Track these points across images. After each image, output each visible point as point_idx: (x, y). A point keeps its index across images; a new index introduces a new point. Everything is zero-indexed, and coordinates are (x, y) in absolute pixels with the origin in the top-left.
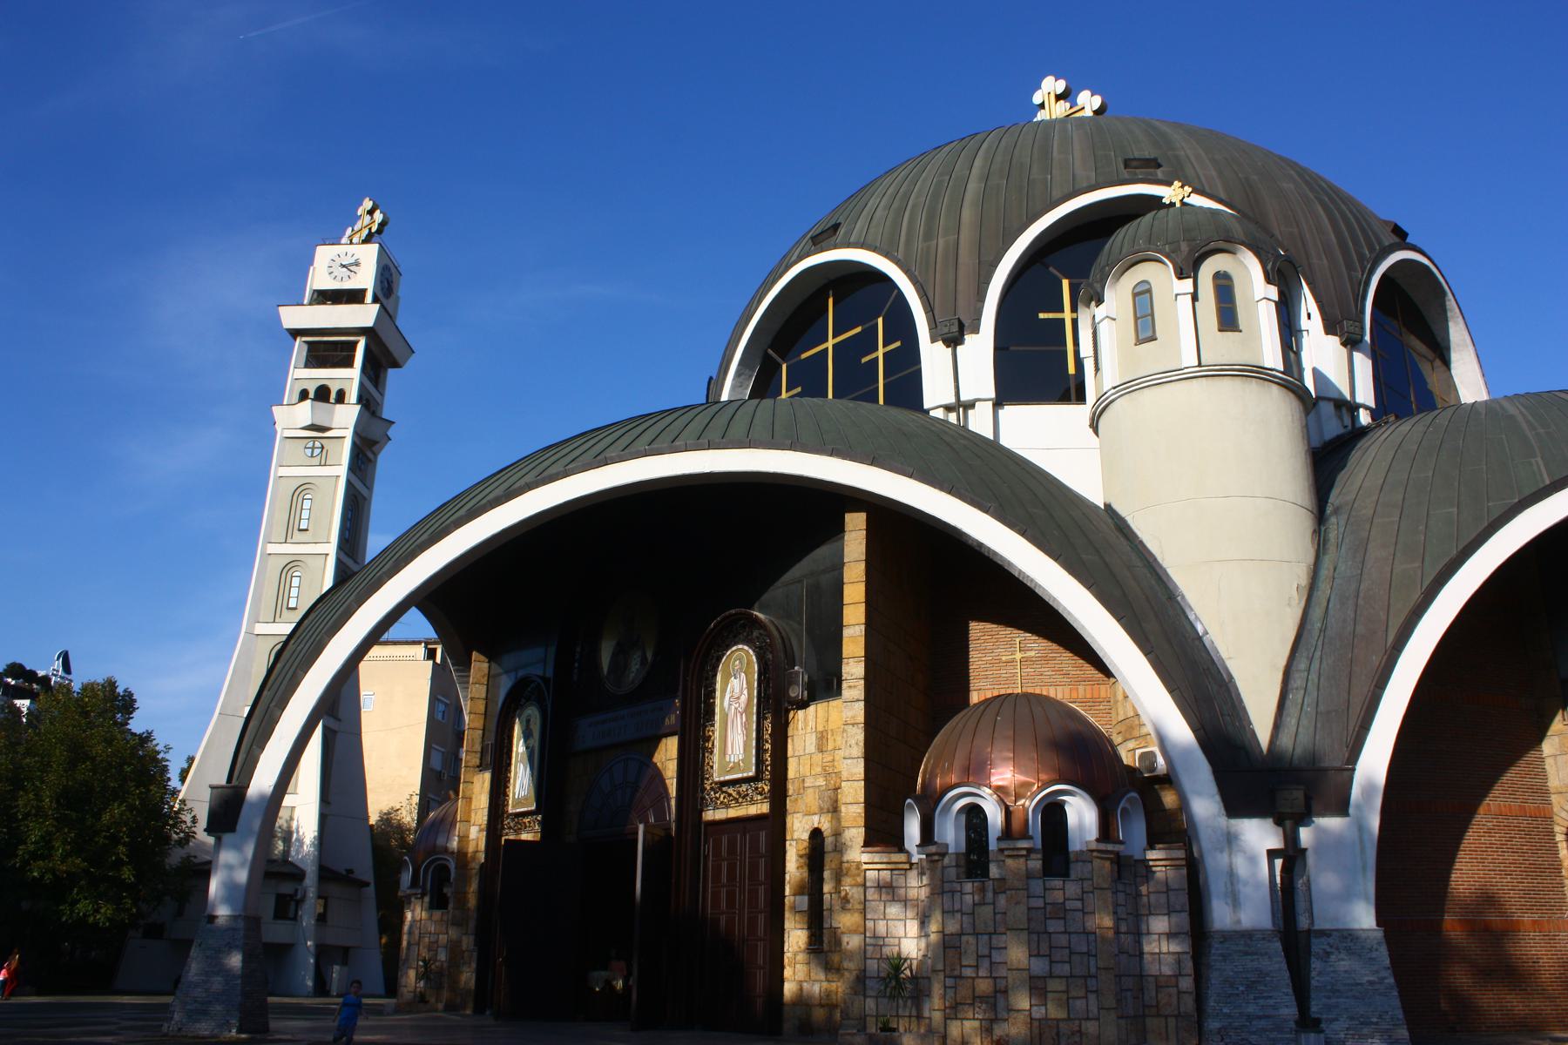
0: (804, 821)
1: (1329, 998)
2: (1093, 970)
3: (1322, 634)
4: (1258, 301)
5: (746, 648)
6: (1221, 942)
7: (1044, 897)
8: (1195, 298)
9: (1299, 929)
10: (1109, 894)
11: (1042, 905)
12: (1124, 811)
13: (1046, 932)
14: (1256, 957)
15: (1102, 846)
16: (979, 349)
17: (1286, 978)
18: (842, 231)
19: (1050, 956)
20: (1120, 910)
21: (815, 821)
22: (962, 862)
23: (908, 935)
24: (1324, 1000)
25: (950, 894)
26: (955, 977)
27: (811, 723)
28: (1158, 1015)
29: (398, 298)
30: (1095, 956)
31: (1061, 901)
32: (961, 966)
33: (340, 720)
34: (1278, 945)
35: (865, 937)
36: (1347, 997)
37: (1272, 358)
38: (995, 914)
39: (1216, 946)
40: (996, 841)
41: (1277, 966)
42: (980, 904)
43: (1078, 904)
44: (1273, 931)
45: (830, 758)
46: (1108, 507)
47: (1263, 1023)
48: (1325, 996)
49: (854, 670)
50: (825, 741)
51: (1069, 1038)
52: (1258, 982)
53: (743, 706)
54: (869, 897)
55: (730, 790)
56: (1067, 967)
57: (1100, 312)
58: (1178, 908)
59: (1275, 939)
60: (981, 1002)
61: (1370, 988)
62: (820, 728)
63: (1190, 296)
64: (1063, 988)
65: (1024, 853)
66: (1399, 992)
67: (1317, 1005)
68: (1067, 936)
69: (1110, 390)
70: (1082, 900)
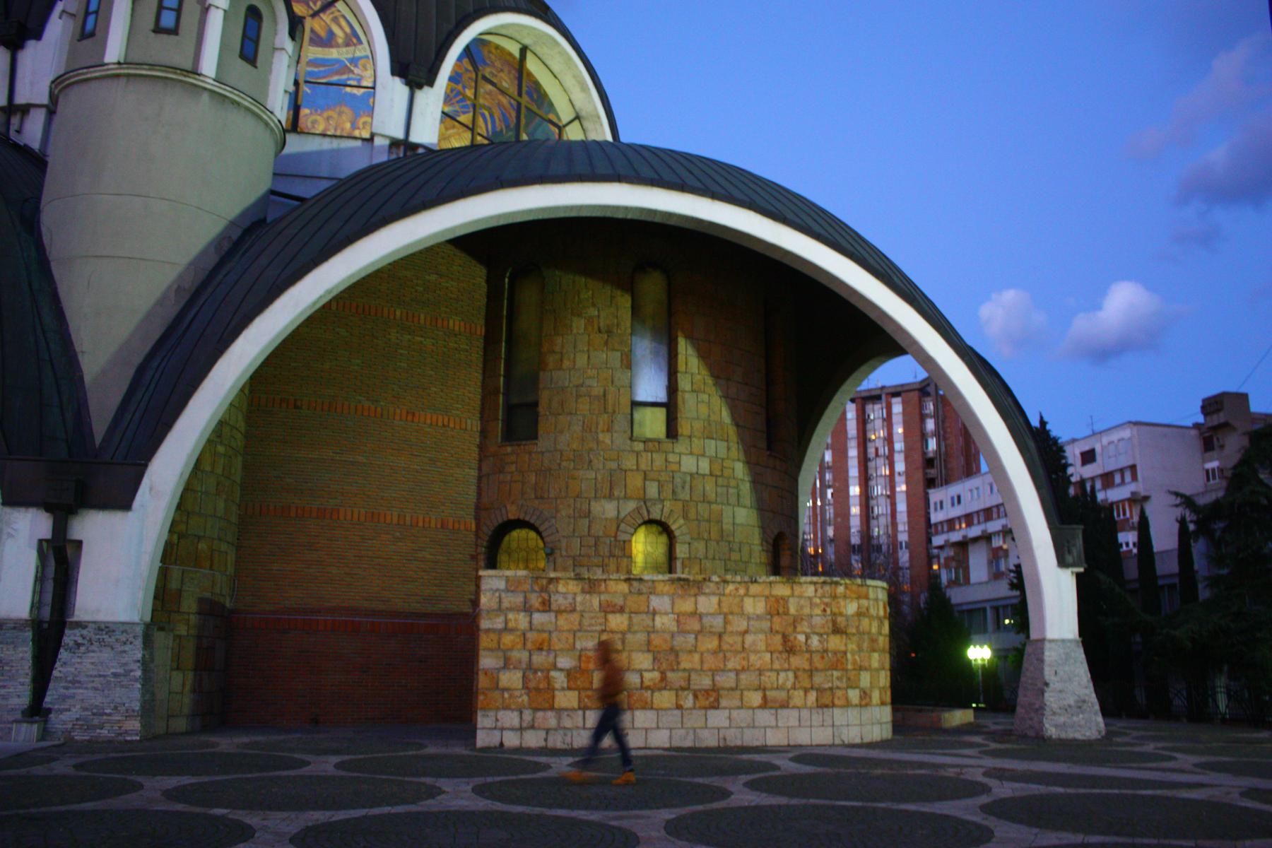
1: (67, 688)
17: (27, 667)
24: (63, 691)
34: (29, 634)
36: (86, 688)
61: (112, 680)
66: (143, 685)
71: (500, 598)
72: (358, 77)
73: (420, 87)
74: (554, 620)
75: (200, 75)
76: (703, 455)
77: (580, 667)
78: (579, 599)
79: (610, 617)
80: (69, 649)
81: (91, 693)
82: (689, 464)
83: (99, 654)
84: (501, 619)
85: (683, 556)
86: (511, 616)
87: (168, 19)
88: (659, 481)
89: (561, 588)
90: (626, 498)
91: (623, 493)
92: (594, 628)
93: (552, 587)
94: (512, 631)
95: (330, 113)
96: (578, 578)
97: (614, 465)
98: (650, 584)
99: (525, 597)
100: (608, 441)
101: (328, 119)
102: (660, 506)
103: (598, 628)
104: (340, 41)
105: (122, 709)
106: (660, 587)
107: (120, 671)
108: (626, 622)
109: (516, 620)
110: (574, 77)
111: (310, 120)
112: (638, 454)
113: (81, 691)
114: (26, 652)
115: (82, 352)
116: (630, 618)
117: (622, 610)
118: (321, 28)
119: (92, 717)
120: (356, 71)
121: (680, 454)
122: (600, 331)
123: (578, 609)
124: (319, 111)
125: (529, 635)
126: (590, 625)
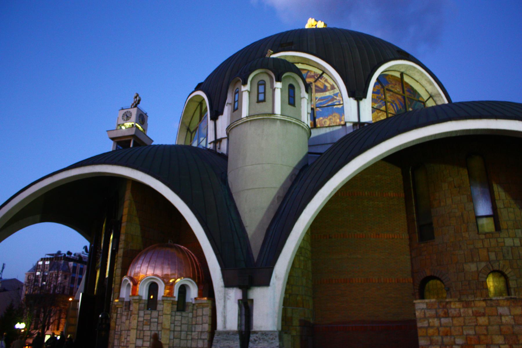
10: (169, 316)
14: (229, 341)
19: (143, 339)
29: (147, 124)
31: (149, 318)
34: (238, 337)
35: (115, 331)
41: (236, 345)
43: (156, 320)
54: (118, 317)
58: (205, 322)
59: (237, 334)
65: (137, 301)
68: (150, 332)
71: (424, 312)
72: (339, 101)
73: (361, 99)
74: (451, 321)
75: (275, 114)
76: (516, 237)
77: (467, 343)
78: (462, 310)
79: (479, 318)
80: (252, 342)
82: (509, 242)
83: (263, 344)
84: (426, 322)
85: (514, 286)
86: (430, 320)
87: (261, 97)
88: (495, 252)
89: (453, 306)
90: (480, 261)
91: (479, 259)
92: (471, 324)
93: (448, 306)
94: (433, 327)
95: (331, 117)
96: (460, 301)
97: (472, 247)
98: (496, 301)
99: (436, 312)
100: (468, 236)
101: (330, 119)
102: (498, 264)
103: (474, 324)
104: (329, 88)
106: (501, 303)
108: (487, 321)
109: (433, 322)
110: (426, 80)
111: (323, 122)
112: (482, 240)
114: (237, 343)
115: (247, 226)
116: (489, 319)
117: (484, 315)
118: (321, 85)
120: (337, 98)
121: (504, 238)
122: (455, 187)
123: (462, 315)
124: (326, 117)
125: (440, 329)
126: (469, 323)
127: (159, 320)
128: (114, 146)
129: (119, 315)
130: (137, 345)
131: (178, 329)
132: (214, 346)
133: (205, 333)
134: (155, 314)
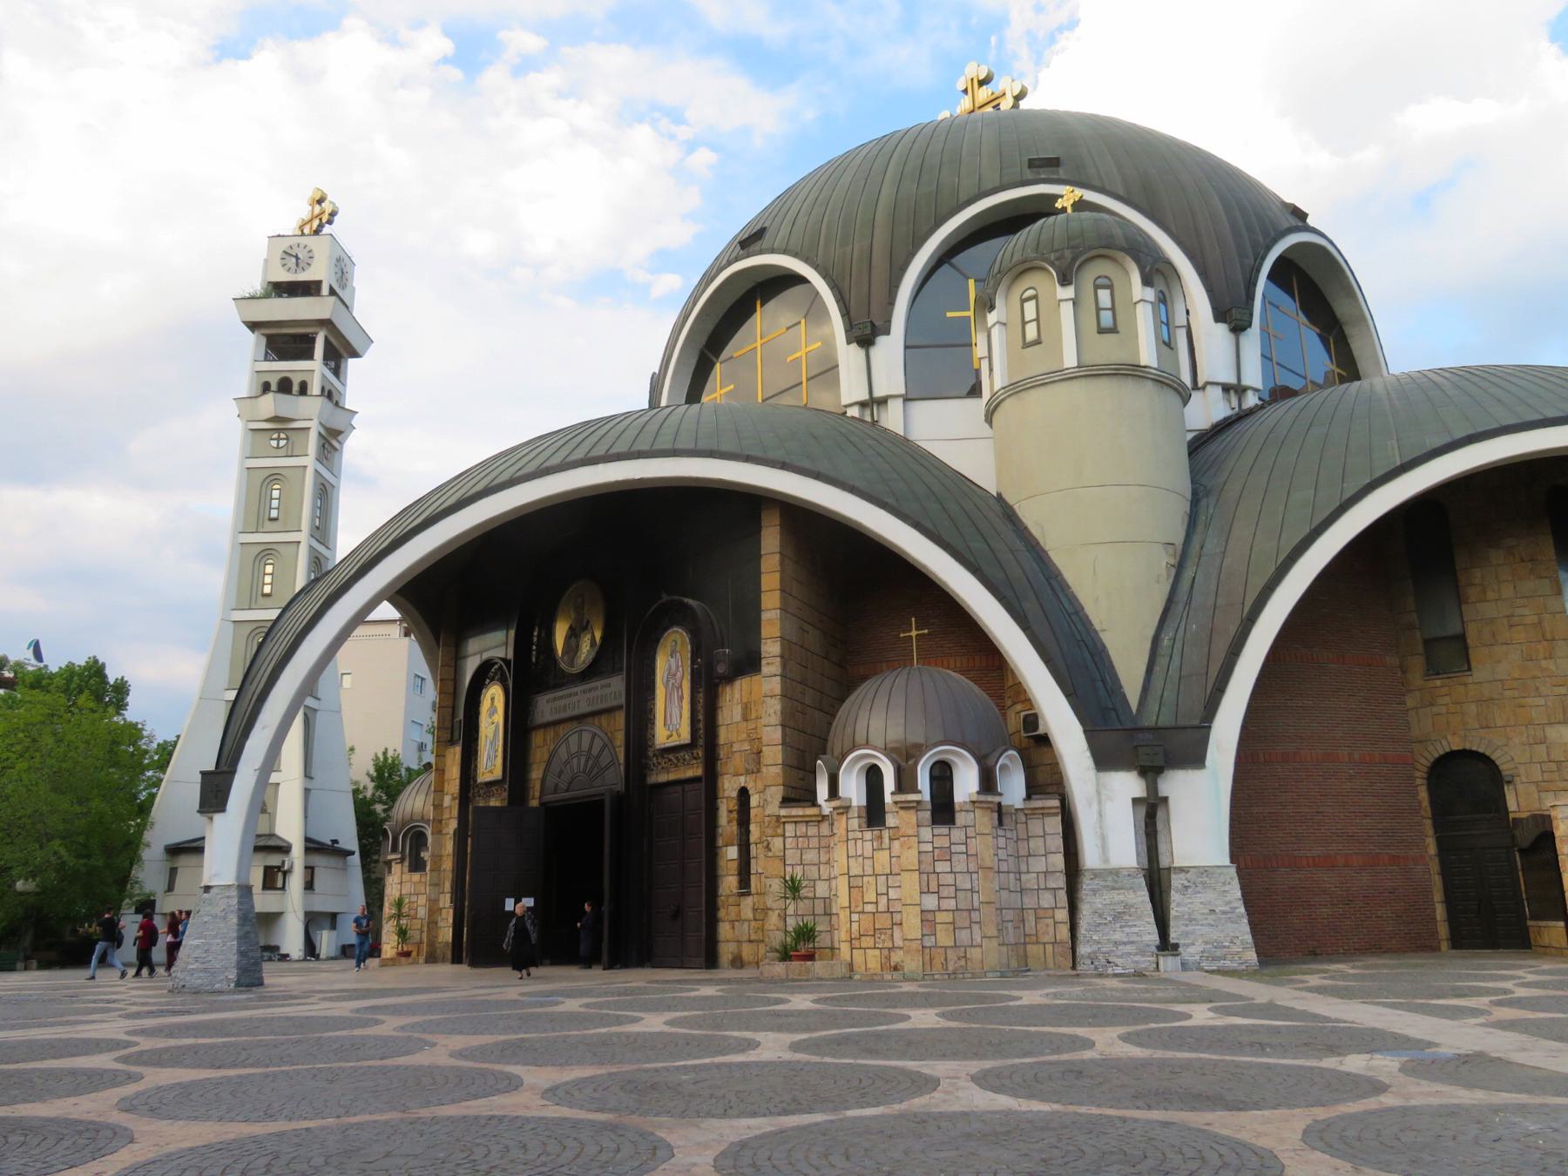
0: (733, 782)
1: (1187, 925)
2: (976, 904)
3: (1187, 607)
4: (1135, 303)
5: (680, 630)
6: (1092, 879)
7: (932, 842)
8: (1075, 302)
9: (1161, 867)
11: (931, 850)
12: (1004, 767)
13: (934, 872)
14: (1122, 891)
15: (982, 798)
16: (890, 349)
18: (768, 236)
19: (938, 892)
20: (1000, 851)
21: (742, 781)
22: (864, 814)
23: (822, 878)
24: (1183, 928)
25: (853, 841)
26: (859, 913)
27: (737, 696)
28: (1038, 942)
29: (354, 288)
30: (978, 892)
31: (948, 845)
32: (864, 903)
33: (319, 699)
34: (1142, 882)
36: (1202, 925)
37: (1147, 355)
38: (891, 857)
39: (1088, 882)
40: (890, 796)
42: (879, 849)
43: (963, 848)
44: (1138, 868)
45: (754, 726)
46: (999, 495)
47: (1129, 948)
48: (1183, 924)
49: (771, 649)
50: (749, 710)
51: (956, 963)
52: (1124, 913)
53: (678, 681)
55: (671, 756)
56: (953, 902)
57: (992, 318)
58: (1053, 849)
60: (881, 934)
61: (1222, 916)
62: (745, 700)
63: (1071, 302)
64: (951, 920)
65: (915, 805)
67: (1175, 932)
68: (953, 875)
69: (1000, 390)
70: (966, 844)
80: (1177, 891)
81: (1207, 929)
105: (1238, 943)
107: (1227, 908)
113: (1199, 927)
114: (1144, 896)
119: (1214, 950)
122: (1523, 561)
127: (969, 848)
128: (257, 345)
129: (789, 841)
130: (924, 908)
131: (1004, 867)
132: (1088, 902)
133: (1058, 874)
134: (957, 835)
